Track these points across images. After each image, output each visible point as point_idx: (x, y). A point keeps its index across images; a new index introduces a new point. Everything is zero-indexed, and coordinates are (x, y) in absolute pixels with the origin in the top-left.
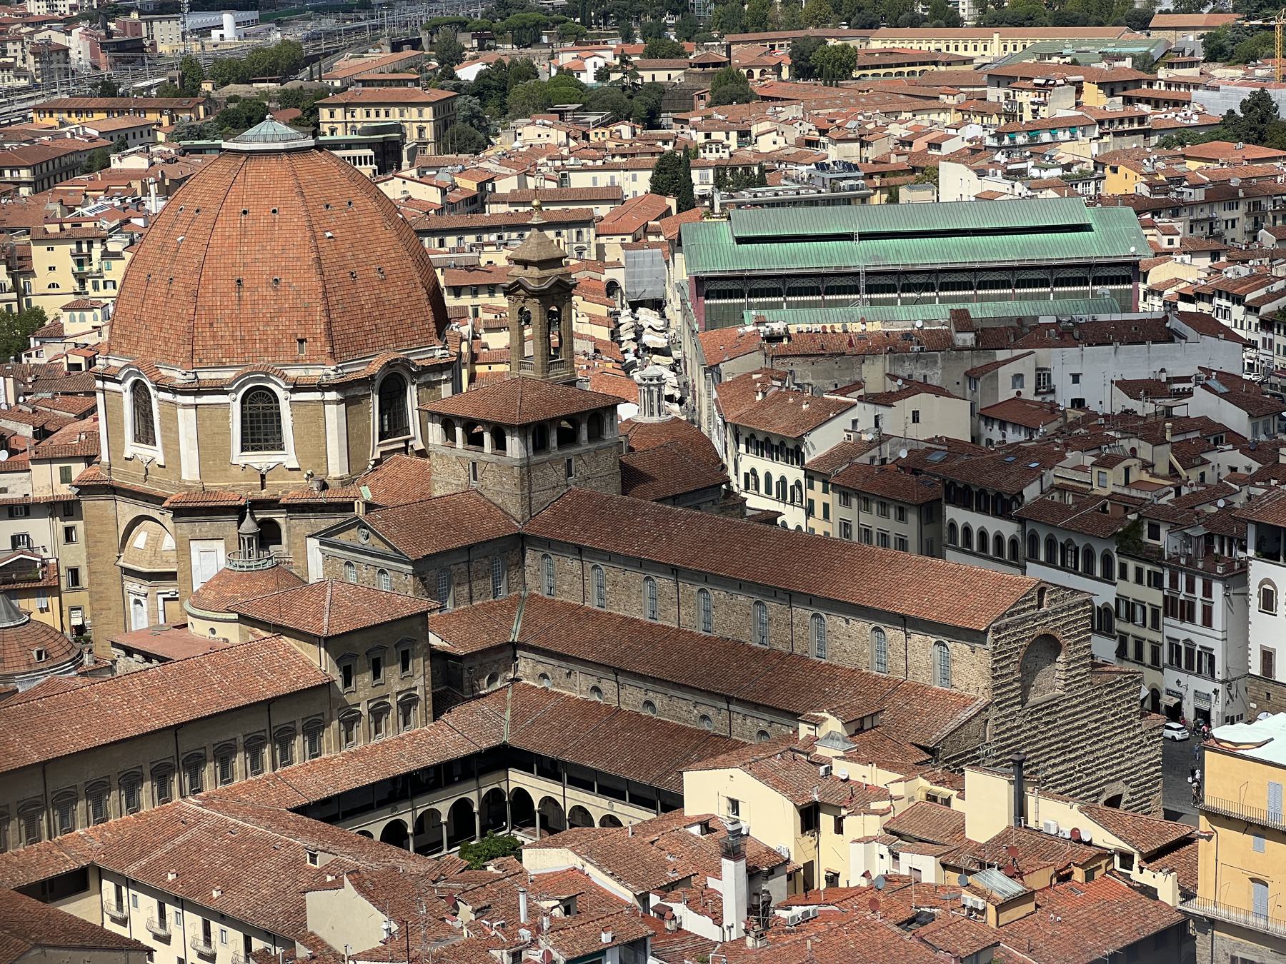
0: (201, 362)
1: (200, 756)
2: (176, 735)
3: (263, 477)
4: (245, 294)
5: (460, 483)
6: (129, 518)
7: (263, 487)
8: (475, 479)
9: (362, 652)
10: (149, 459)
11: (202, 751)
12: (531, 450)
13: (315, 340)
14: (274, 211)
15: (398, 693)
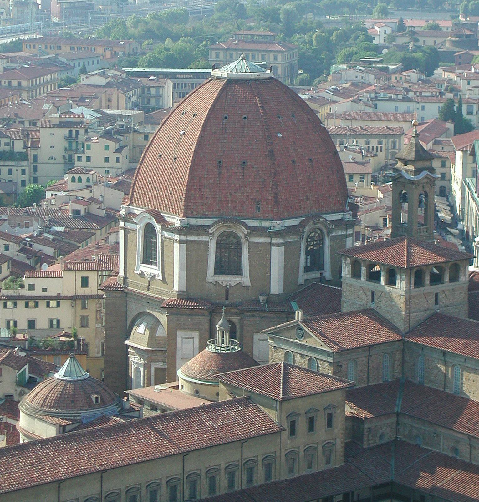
0: (192, 212)
1: (198, 475)
2: (184, 459)
3: (227, 291)
4: (224, 171)
5: (362, 304)
6: (135, 313)
7: (227, 299)
8: (373, 300)
9: (302, 412)
10: (152, 275)
11: (199, 472)
12: (412, 285)
13: (267, 203)
14: (245, 118)
15: (323, 442)
